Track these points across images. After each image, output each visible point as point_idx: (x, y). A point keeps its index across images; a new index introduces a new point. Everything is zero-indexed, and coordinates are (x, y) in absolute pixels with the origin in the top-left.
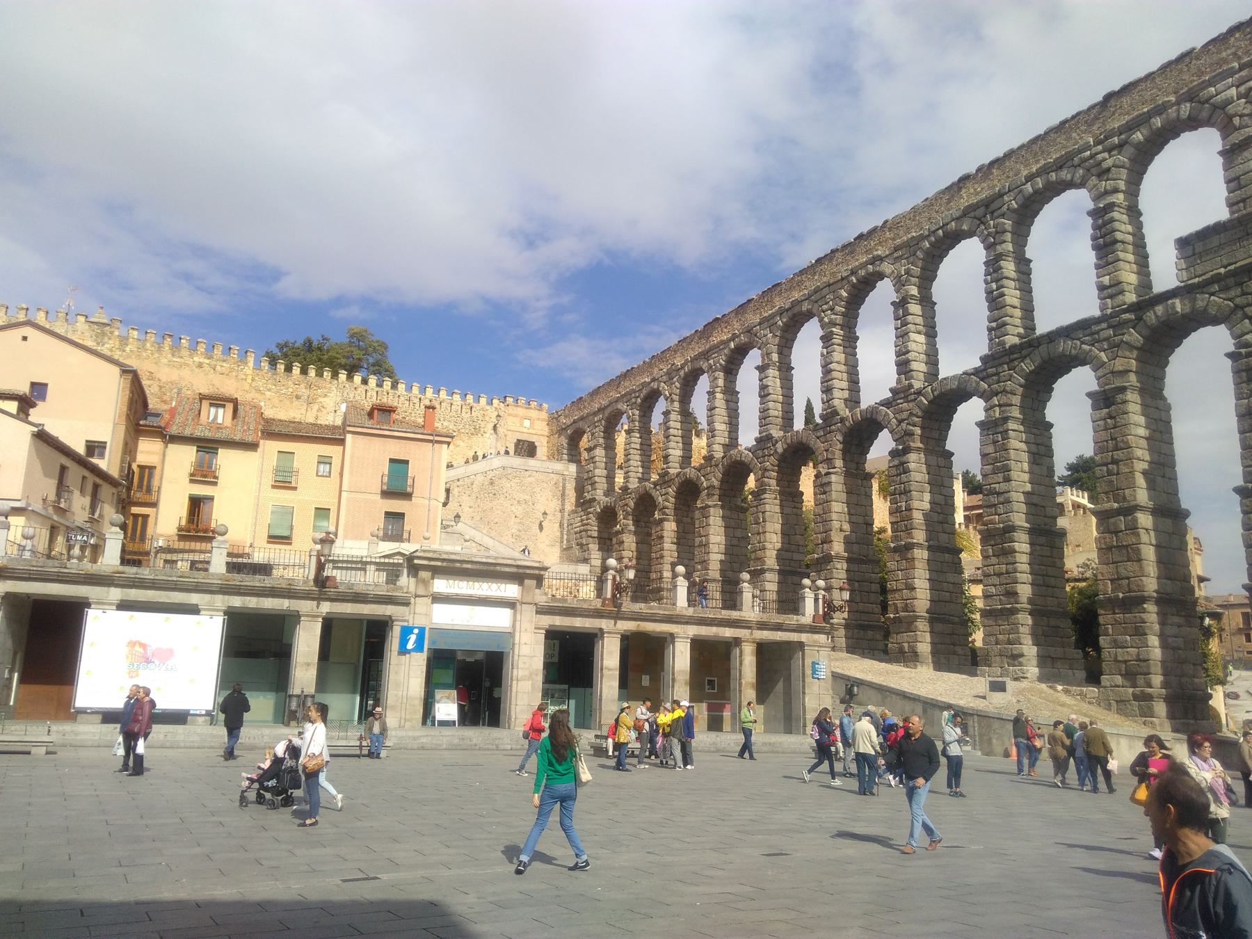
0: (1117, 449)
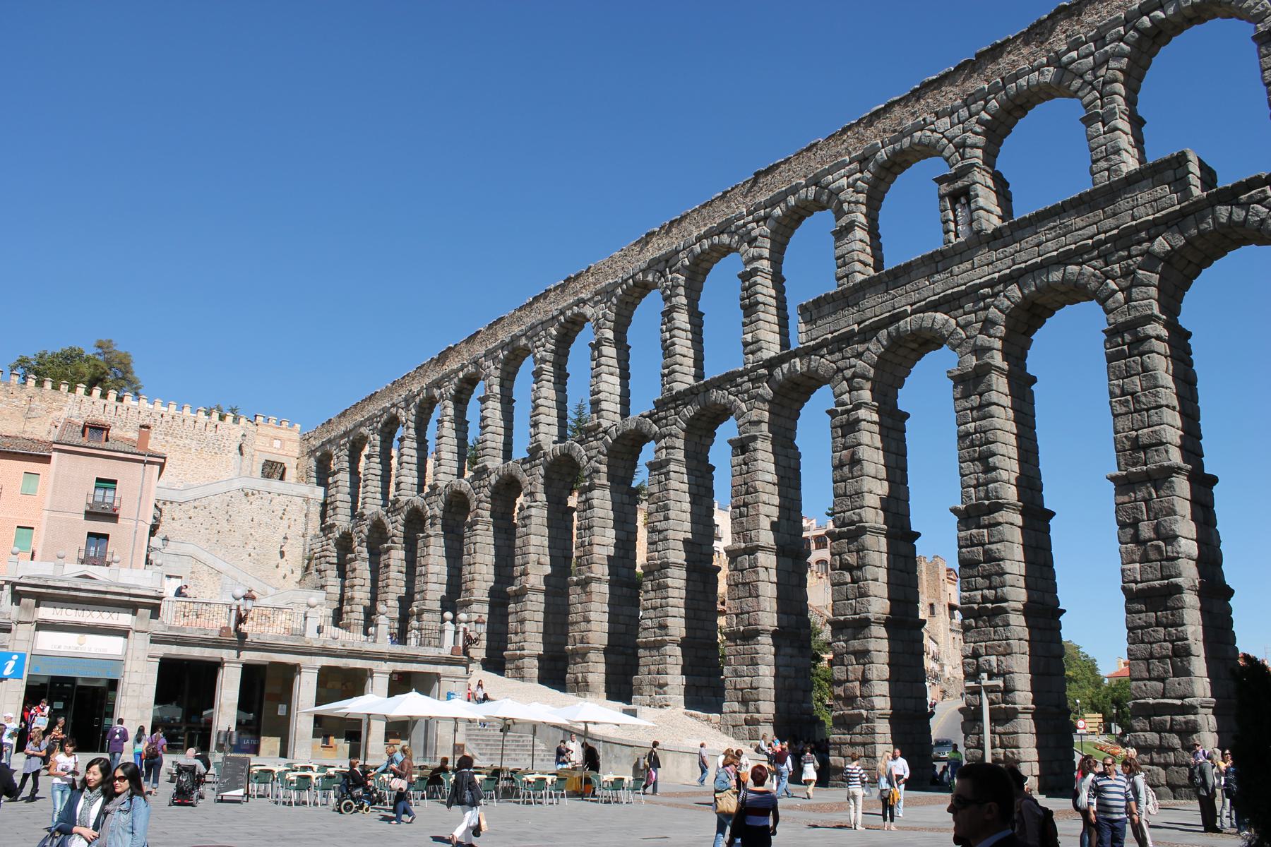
0: (747, 493)
